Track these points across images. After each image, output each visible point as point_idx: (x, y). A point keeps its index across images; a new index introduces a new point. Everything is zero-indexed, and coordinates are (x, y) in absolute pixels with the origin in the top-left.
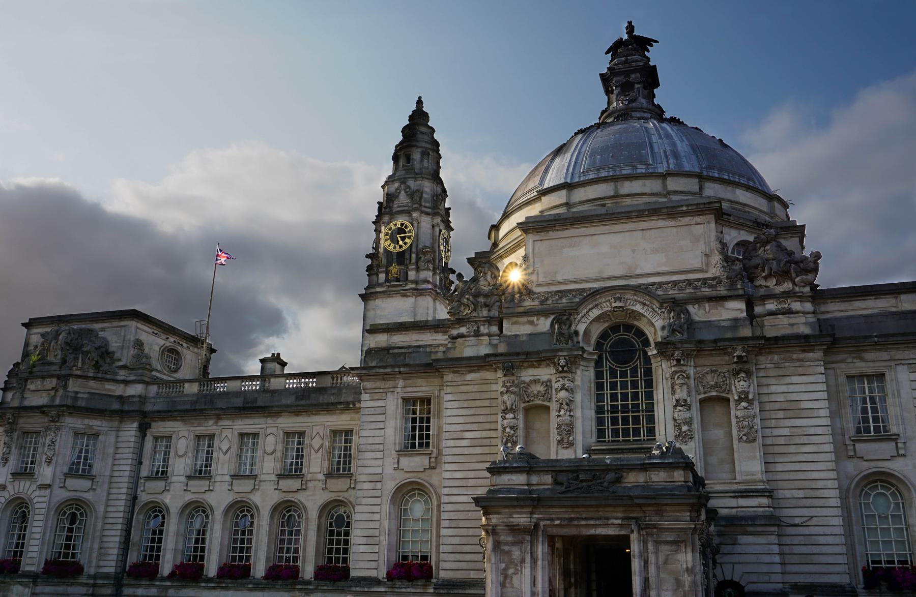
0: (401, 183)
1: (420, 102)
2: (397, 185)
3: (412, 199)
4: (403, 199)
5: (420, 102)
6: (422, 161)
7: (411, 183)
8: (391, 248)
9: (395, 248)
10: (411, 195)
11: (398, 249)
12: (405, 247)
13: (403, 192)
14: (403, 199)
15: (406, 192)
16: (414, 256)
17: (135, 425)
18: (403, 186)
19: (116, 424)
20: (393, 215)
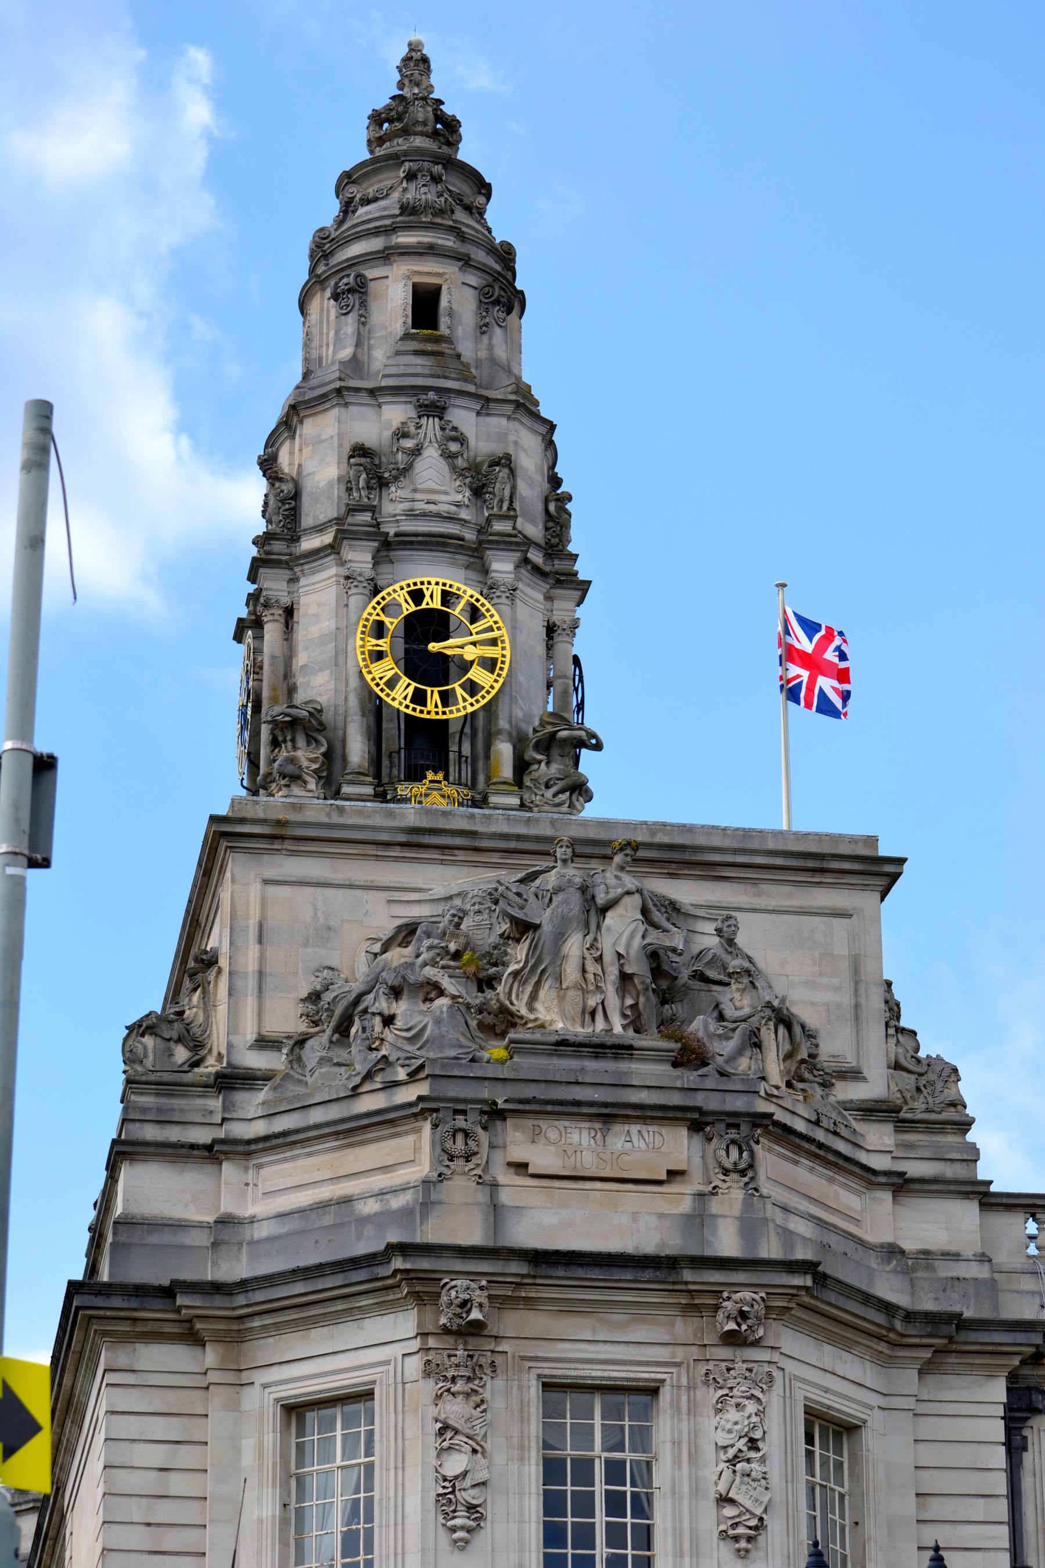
0: (435, 410)
1: (416, 63)
2: (397, 413)
3: (478, 492)
4: (433, 484)
5: (416, 63)
6: (483, 329)
7: (462, 417)
8: (400, 697)
9: (419, 698)
10: (482, 477)
11: (433, 709)
12: (464, 706)
13: (431, 454)
14: (433, 484)
15: (449, 457)
16: (504, 750)
17: (998, 1391)
18: (431, 426)
19: (907, 1379)
20: (389, 547)
